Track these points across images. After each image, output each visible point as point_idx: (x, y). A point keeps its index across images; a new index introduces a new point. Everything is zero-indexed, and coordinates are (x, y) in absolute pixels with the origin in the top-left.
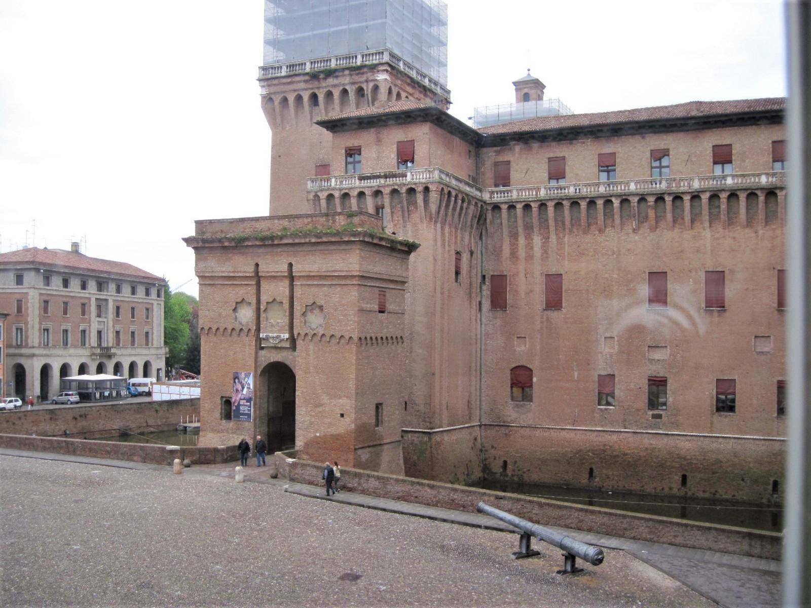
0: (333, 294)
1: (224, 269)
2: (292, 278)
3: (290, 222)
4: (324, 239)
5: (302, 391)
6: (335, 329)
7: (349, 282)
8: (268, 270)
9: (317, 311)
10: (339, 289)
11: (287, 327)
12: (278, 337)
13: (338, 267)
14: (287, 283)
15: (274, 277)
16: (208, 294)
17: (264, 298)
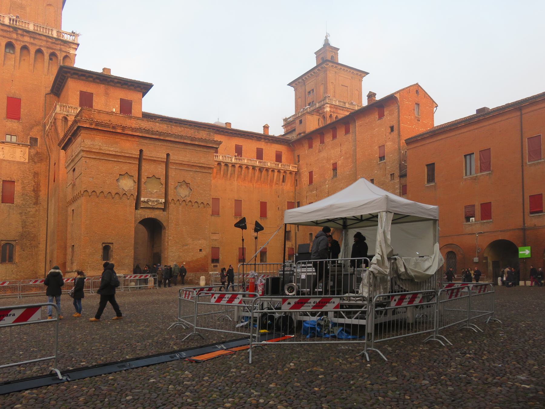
0: (197, 177)
1: (112, 149)
2: (167, 163)
3: (168, 127)
4: (197, 143)
5: (174, 236)
6: (197, 198)
7: (204, 171)
8: (151, 155)
9: (184, 186)
10: (200, 174)
11: (164, 195)
12: (156, 201)
13: (202, 161)
14: (164, 166)
15: (155, 161)
16: (92, 166)
17: (144, 174)
